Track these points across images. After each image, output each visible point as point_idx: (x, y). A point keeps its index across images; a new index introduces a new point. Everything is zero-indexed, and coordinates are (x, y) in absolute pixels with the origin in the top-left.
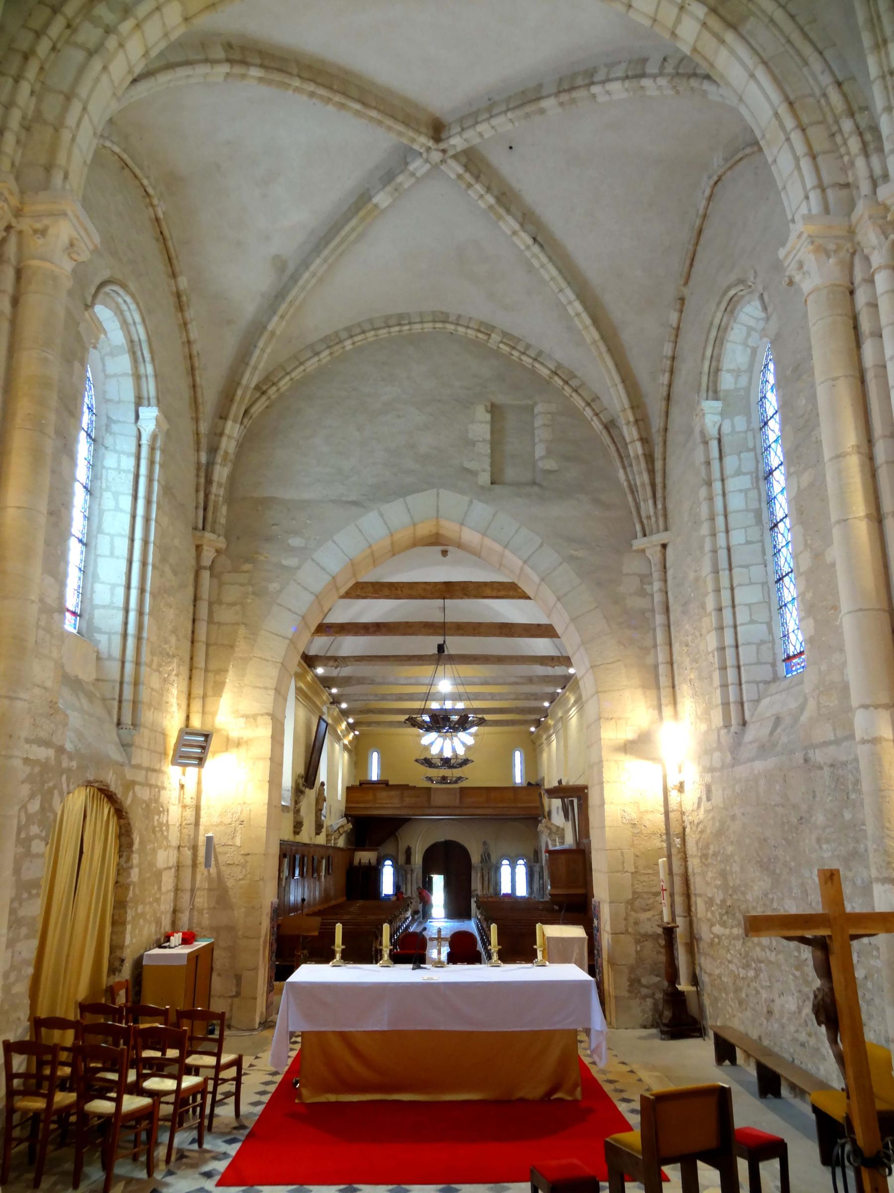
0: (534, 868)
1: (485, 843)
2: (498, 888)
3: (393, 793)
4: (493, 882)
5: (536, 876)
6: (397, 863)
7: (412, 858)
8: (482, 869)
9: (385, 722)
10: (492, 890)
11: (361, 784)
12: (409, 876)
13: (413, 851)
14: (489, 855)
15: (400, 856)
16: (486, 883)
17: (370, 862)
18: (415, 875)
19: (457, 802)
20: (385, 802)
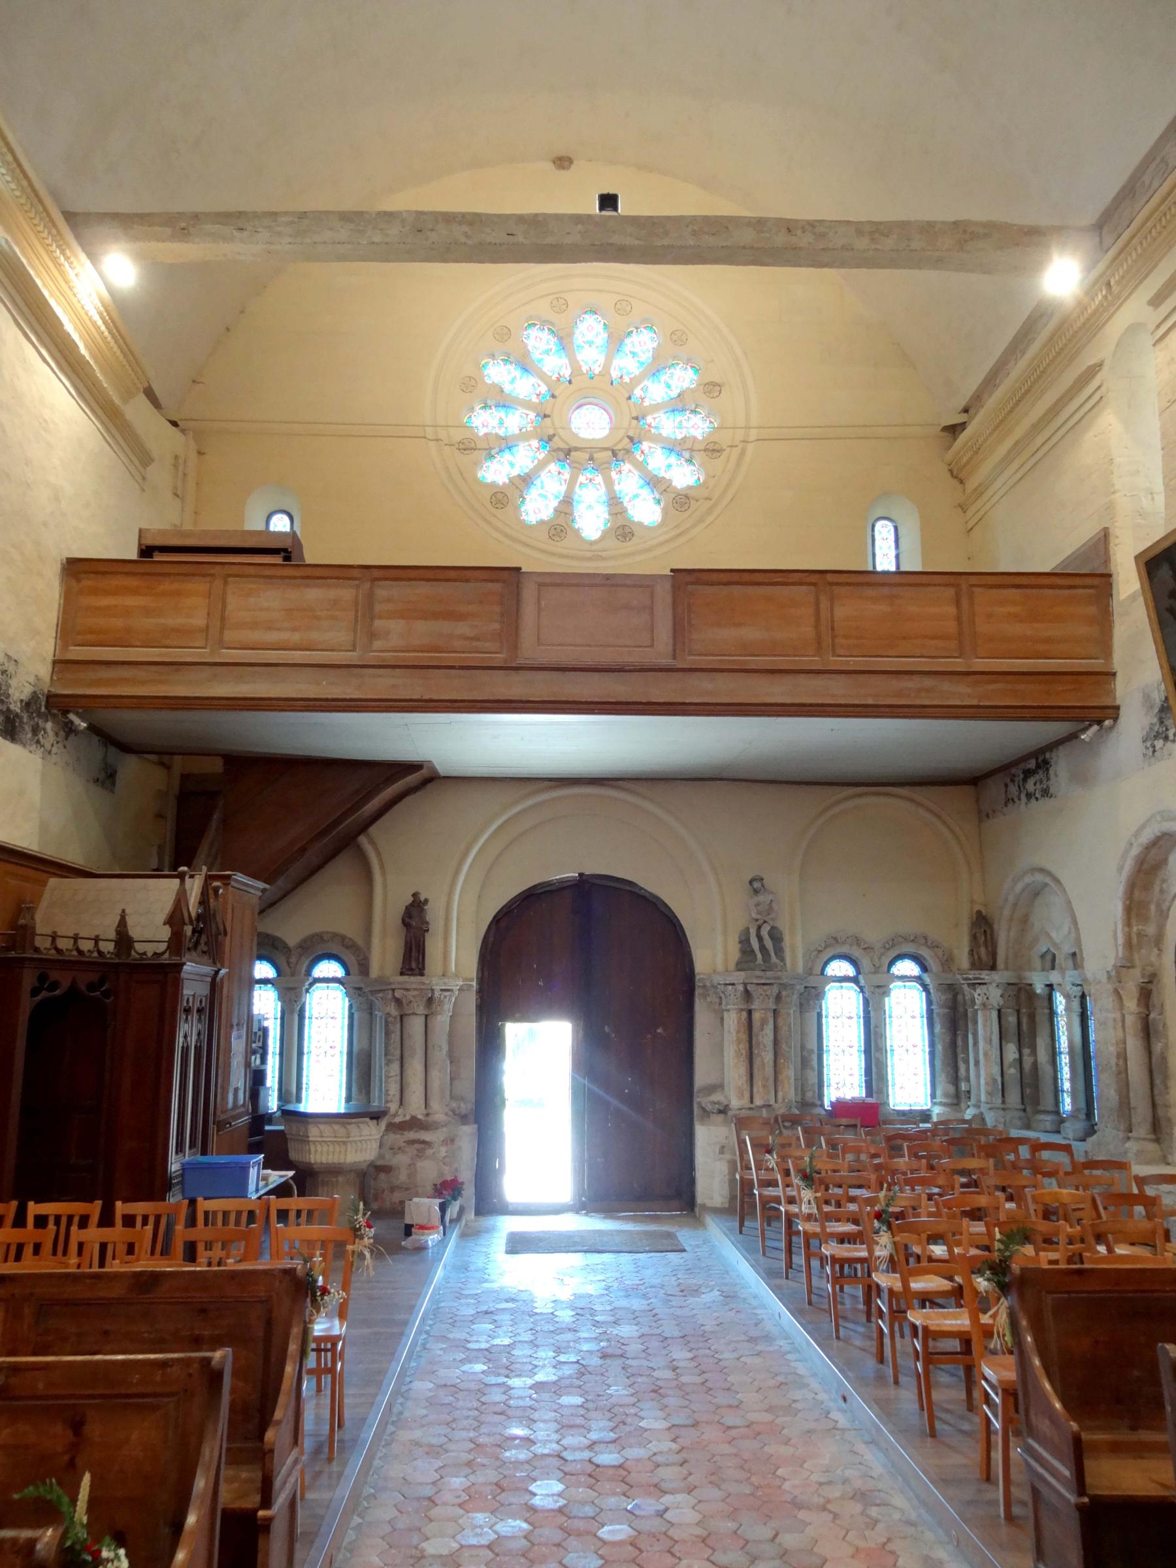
0: (978, 995)
1: (756, 885)
2: (812, 1078)
3: (314, 594)
4: (792, 1052)
5: (985, 1028)
6: (364, 968)
7: (433, 947)
8: (747, 995)
9: (274, 215)
10: (789, 1092)
11: (147, 551)
12: (416, 1025)
13: (434, 913)
14: (776, 936)
15: (376, 940)
16: (766, 1056)
17: (124, 940)
18: (442, 1021)
19: (661, 650)
20: (273, 637)
